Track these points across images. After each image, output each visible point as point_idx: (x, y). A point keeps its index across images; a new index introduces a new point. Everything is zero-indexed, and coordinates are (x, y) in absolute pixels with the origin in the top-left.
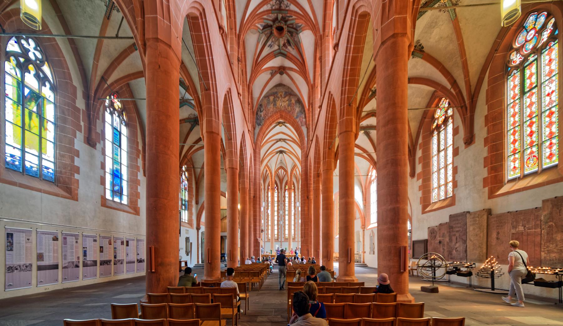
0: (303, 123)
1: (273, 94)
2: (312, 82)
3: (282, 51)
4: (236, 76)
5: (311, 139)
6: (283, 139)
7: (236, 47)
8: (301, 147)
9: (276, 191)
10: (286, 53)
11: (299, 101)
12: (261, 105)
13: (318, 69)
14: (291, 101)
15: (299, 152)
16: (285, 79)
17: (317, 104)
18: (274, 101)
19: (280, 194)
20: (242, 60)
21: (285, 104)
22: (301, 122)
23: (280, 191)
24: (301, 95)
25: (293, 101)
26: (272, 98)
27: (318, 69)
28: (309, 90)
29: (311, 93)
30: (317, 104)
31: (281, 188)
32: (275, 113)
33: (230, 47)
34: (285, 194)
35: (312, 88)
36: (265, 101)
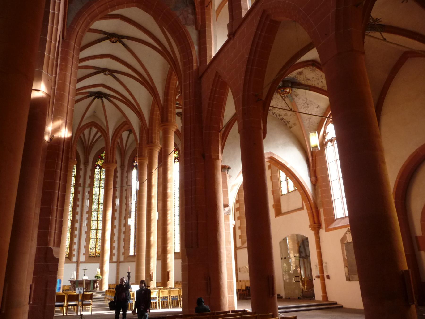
9: (75, 167)
19: (82, 173)
23: (82, 166)
31: (86, 162)
34: (93, 174)
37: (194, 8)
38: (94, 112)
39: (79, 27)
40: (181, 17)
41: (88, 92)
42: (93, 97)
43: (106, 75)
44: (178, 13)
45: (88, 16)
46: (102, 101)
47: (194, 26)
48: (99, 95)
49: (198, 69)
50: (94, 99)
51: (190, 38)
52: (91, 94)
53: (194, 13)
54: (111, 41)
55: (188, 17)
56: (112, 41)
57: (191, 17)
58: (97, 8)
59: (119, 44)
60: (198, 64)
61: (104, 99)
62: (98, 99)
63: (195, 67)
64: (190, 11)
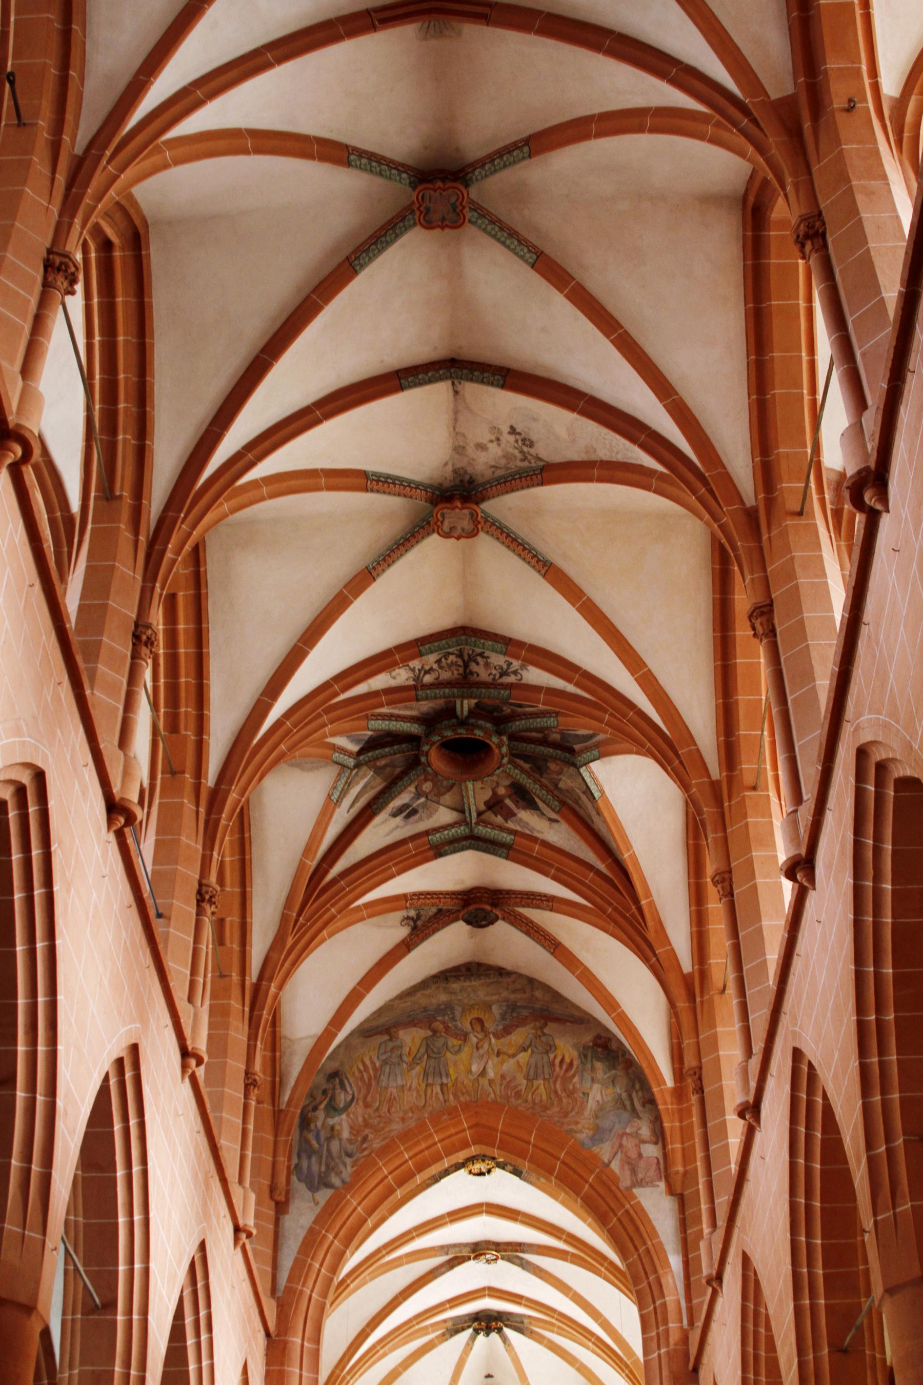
0: (647, 1170)
1: (430, 1013)
2: (687, 965)
3: (481, 830)
4: (179, 971)
5: (707, 1269)
6: (497, 1246)
7: (191, 841)
8: (640, 1279)
10: (508, 838)
11: (611, 1050)
12: (334, 1075)
13: (718, 928)
14: (550, 1048)
15: (623, 1314)
16: (506, 944)
17: (733, 1092)
18: (431, 1051)
20: (222, 897)
21: (509, 1065)
22: (632, 1166)
24: (623, 1020)
25: (566, 1047)
26: (411, 1038)
27: (718, 928)
28: (672, 1003)
29: (686, 1020)
30: (733, 1092)
32: (435, 1119)
33: (158, 844)
35: (687, 996)
36: (370, 1054)
37: (657, 1121)
38: (489, 1376)
39: (310, 1283)
40: (615, 1166)
41: (445, 1321)
42: (470, 1331)
43: (488, 1261)
44: (605, 1151)
45: (335, 1237)
46: (505, 1339)
47: (662, 1185)
48: (487, 1322)
49: (685, 1340)
50: (473, 1339)
51: (654, 1233)
52: (456, 1327)
53: (659, 1136)
54: (470, 1172)
55: (640, 1156)
56: (476, 1171)
57: (651, 1151)
58: (359, 1204)
59: (498, 1172)
60: (685, 1322)
61: (507, 1331)
62: (488, 1335)
63: (674, 1337)
64: (645, 1131)
